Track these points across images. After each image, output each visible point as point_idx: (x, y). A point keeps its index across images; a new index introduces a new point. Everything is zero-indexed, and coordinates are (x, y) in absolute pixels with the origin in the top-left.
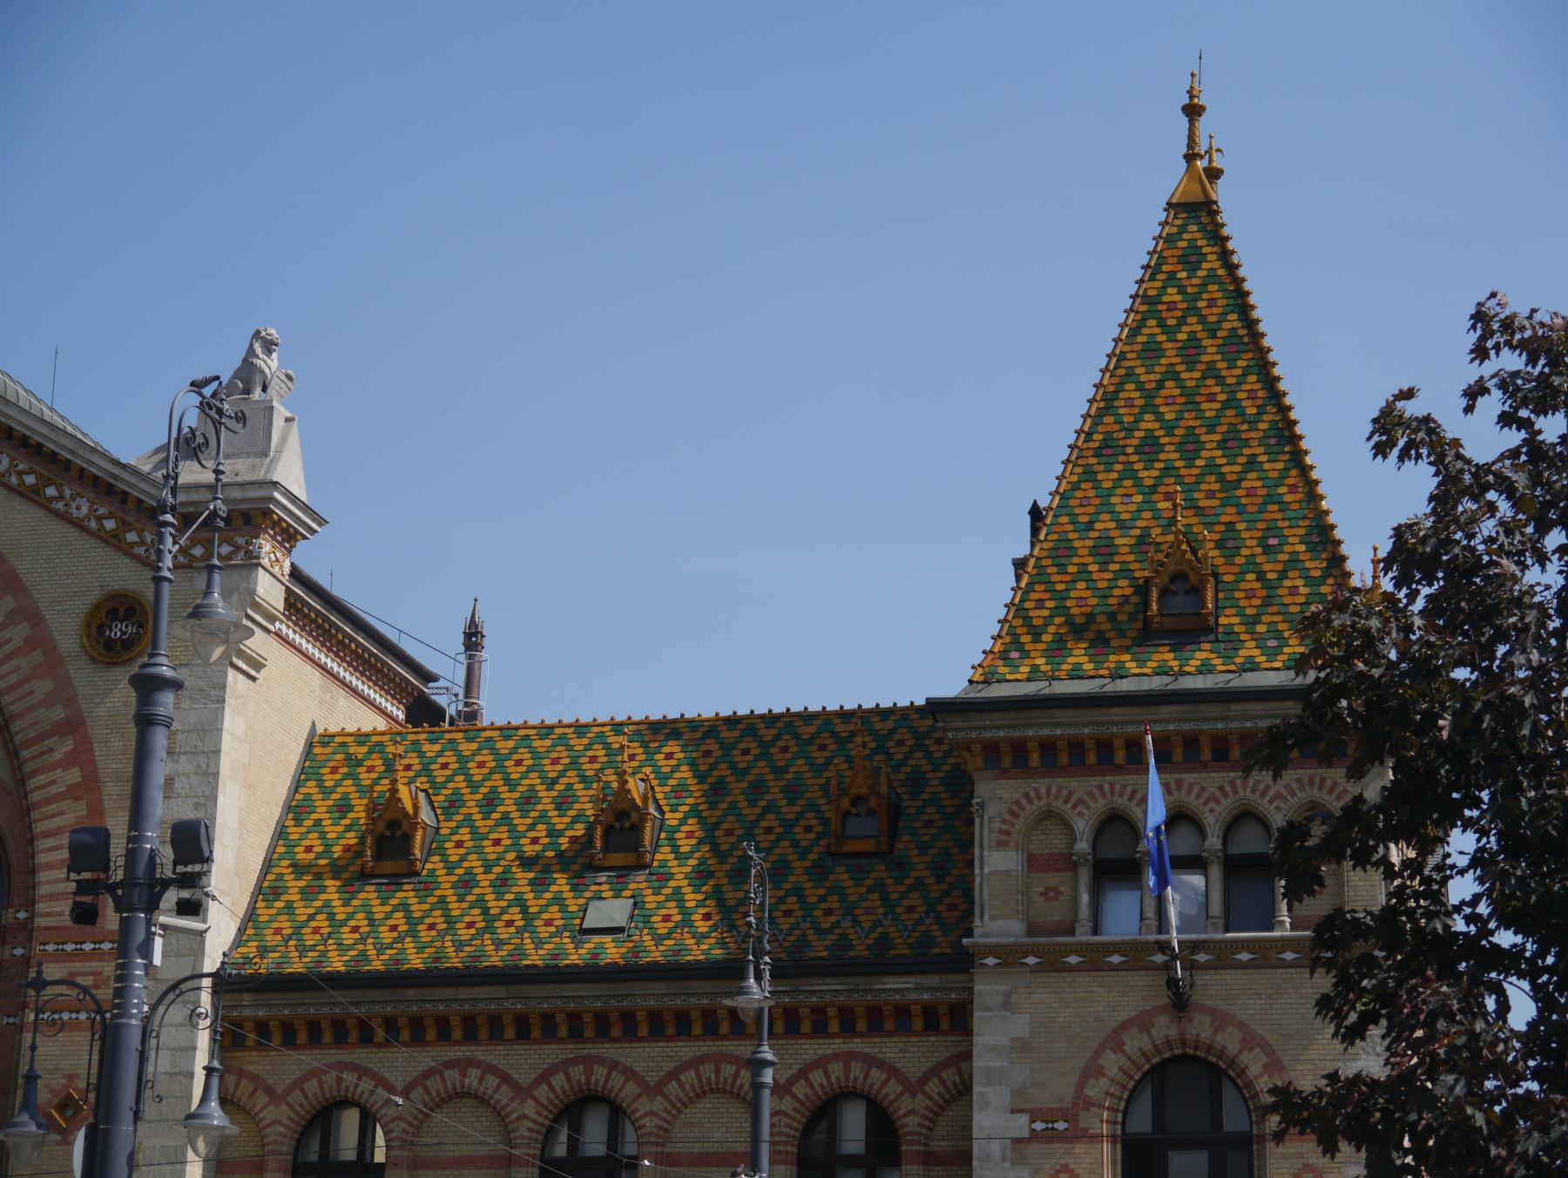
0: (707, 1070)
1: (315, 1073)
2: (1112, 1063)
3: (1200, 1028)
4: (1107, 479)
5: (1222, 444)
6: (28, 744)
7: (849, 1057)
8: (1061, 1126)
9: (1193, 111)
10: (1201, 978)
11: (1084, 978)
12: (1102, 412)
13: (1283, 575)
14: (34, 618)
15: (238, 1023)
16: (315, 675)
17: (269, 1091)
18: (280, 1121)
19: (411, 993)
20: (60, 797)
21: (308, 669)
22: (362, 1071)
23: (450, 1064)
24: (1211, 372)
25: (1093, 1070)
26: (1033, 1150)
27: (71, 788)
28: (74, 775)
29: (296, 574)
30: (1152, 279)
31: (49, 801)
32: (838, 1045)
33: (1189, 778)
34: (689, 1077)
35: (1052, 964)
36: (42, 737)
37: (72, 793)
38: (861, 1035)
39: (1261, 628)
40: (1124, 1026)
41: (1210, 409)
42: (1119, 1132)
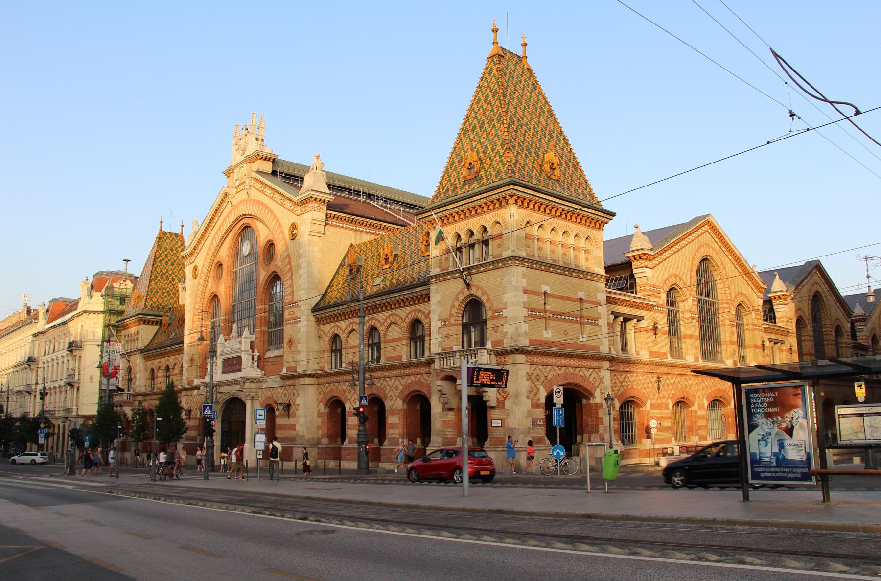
0: (391, 317)
1: (331, 329)
2: (457, 303)
3: (474, 291)
4: (464, 140)
5: (488, 123)
7: (415, 310)
8: (447, 323)
9: (495, 31)
10: (473, 276)
11: (450, 281)
12: (466, 122)
13: (495, 156)
14: (282, 232)
16: (352, 232)
17: (325, 334)
18: (327, 339)
19: (340, 307)
21: (348, 231)
22: (338, 327)
23: (351, 323)
24: (490, 103)
25: (453, 307)
26: (442, 330)
28: (288, 267)
29: (328, 210)
30: (482, 80)
31: (286, 273)
32: (413, 308)
33: (470, 220)
34: (388, 320)
35: (445, 280)
38: (417, 304)
39: (488, 174)
40: (459, 293)
41: (487, 113)
42: (460, 322)
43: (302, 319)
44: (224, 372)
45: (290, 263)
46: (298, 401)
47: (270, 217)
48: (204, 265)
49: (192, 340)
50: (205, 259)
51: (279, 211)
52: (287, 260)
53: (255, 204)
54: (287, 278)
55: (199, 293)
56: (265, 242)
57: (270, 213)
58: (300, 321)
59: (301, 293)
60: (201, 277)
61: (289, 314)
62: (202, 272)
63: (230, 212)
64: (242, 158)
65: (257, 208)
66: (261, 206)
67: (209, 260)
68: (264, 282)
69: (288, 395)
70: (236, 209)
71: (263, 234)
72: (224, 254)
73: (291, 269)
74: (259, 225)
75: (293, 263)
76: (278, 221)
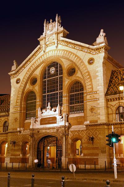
6: (84, 74)
15: (108, 99)
17: (112, 106)
18: (114, 109)
20: (87, 79)
27: (88, 78)
28: (89, 76)
36: (85, 74)
37: (88, 78)
43: (100, 99)
44: (41, 124)
45: (89, 75)
46: (100, 136)
47: (73, 56)
48: (24, 78)
49: (15, 111)
50: (25, 75)
51: (80, 54)
52: (87, 74)
53: (61, 51)
54: (88, 81)
55: (21, 90)
56: (68, 67)
57: (72, 55)
58: (99, 100)
59: (98, 88)
60: (22, 83)
61: (90, 97)
62: (23, 81)
63: (43, 55)
64: (51, 32)
65: (63, 53)
66: (65, 52)
67: (28, 76)
68: (69, 84)
69: (91, 133)
70: (47, 54)
71: (66, 65)
72: (38, 73)
73: (90, 77)
74: (63, 60)
75: (92, 74)
76: (78, 57)
